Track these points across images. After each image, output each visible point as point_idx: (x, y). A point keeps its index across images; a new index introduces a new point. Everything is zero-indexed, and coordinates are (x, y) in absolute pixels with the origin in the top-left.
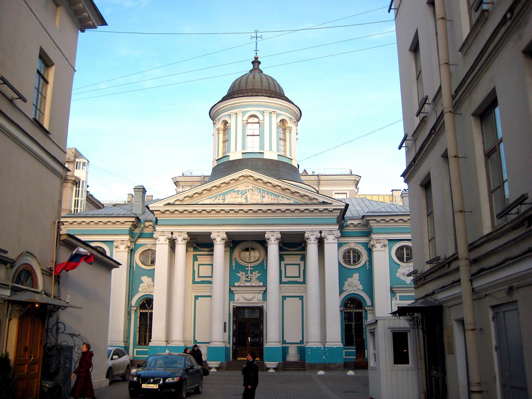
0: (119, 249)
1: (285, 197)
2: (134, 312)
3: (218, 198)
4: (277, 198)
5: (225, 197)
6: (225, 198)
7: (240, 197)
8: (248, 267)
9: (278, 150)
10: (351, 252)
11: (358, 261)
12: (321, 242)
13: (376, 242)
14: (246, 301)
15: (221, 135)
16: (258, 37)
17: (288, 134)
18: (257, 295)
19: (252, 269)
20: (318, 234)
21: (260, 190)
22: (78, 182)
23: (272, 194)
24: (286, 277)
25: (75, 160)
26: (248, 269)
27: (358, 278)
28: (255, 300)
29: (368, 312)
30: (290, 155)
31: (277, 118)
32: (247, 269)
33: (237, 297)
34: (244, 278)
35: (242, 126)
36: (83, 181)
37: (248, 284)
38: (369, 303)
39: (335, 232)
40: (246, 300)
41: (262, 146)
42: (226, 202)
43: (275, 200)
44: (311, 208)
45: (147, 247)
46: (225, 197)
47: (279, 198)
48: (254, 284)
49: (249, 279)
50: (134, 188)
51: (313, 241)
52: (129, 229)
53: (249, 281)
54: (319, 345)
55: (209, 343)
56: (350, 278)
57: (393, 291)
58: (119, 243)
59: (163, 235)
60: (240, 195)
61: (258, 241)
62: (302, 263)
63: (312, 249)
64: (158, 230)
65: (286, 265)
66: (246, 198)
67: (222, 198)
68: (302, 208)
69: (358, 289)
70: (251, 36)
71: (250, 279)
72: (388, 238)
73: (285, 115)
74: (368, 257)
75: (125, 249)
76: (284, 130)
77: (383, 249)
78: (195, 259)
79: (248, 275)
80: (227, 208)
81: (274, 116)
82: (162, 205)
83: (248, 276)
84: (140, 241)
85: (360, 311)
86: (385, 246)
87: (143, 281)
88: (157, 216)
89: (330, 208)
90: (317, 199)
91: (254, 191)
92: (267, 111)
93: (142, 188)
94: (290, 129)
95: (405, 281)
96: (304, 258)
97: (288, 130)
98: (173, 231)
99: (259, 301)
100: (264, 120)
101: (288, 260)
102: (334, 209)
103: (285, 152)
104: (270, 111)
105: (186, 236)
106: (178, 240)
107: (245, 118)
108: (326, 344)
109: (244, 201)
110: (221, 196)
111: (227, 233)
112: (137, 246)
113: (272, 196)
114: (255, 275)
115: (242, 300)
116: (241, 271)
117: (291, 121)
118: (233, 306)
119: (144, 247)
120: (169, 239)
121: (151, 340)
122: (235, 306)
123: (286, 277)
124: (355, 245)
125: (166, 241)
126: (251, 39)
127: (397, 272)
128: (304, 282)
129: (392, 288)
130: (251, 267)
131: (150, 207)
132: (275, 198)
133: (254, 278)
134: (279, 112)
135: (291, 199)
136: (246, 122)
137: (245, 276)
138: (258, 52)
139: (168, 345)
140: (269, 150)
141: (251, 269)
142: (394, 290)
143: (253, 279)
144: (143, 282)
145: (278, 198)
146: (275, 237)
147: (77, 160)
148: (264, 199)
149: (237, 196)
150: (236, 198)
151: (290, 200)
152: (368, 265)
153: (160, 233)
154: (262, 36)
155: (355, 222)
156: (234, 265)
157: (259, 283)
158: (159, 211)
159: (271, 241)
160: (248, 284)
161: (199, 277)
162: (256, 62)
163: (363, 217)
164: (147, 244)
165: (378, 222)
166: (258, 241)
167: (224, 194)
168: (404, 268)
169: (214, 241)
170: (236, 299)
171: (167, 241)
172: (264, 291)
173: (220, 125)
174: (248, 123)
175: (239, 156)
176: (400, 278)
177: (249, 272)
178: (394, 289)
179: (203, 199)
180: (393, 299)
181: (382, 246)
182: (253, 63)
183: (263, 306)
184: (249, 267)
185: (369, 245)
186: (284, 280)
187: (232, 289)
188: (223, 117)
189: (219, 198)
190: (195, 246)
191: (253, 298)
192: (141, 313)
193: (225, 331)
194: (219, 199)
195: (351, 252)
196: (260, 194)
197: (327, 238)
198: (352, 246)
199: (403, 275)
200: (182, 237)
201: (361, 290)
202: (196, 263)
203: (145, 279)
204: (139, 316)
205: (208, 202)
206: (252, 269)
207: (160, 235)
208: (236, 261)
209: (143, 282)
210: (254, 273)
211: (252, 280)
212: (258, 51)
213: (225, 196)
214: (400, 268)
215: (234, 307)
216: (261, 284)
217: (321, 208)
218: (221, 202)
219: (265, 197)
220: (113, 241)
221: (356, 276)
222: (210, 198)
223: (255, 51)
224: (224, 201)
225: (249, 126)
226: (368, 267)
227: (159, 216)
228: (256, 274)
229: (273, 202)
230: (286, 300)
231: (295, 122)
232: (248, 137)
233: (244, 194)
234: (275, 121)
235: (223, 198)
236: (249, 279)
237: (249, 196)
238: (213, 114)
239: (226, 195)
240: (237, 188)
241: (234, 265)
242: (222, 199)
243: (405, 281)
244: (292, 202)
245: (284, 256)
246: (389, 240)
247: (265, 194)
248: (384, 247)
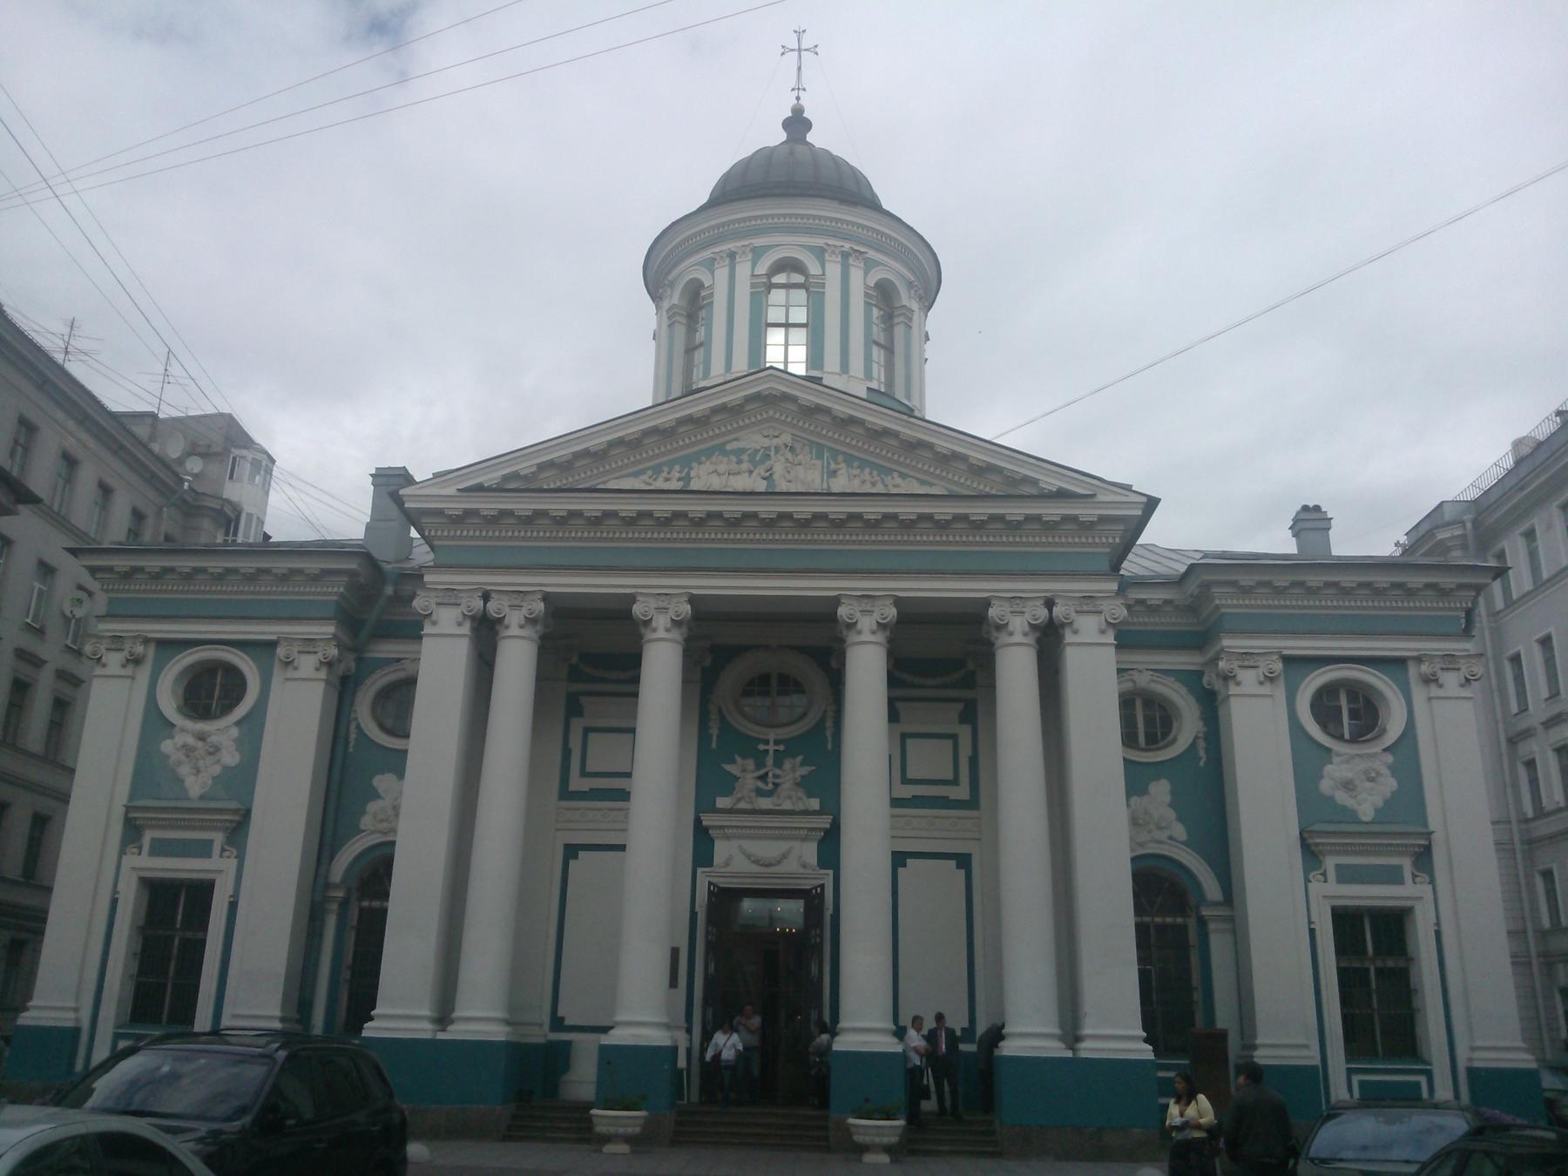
0: (296, 669)
1: (912, 473)
2: (334, 907)
3: (664, 474)
4: (882, 479)
5: (688, 473)
6: (692, 476)
7: (747, 474)
8: (767, 742)
9: (868, 375)
10: (1139, 704)
11: (1164, 737)
13: (1236, 663)
14: (755, 868)
15: (681, 331)
16: (806, 50)
17: (899, 331)
18: (797, 844)
19: (781, 748)
20: (1038, 609)
21: (819, 450)
22: (232, 516)
23: (863, 464)
24: (905, 781)
25: (227, 451)
26: (767, 747)
27: (1168, 799)
28: (790, 866)
29: (1212, 926)
30: (908, 397)
31: (866, 274)
32: (761, 747)
33: (722, 850)
34: (749, 781)
35: (752, 293)
36: (250, 516)
37: (765, 803)
38: (1212, 889)
39: (1105, 606)
40: (757, 862)
41: (815, 356)
42: (694, 486)
43: (874, 484)
44: (1015, 511)
45: (404, 670)
46: (688, 473)
47: (890, 478)
48: (787, 806)
49: (767, 784)
50: (374, 472)
51: (1018, 638)
52: (335, 598)
53: (769, 794)
54: (1055, 1049)
55: (605, 1030)
56: (1139, 796)
57: (1313, 848)
58: (296, 649)
59: (452, 601)
60: (745, 466)
61: (803, 650)
62: (964, 732)
64: (431, 583)
65: (904, 737)
66: (768, 474)
67: (677, 475)
68: (979, 511)
69: (1171, 838)
70: (783, 47)
71: (773, 783)
72: (1286, 652)
73: (892, 270)
74: (1201, 724)
75: (317, 669)
76: (888, 319)
77: (1266, 689)
78: (574, 708)
79: (766, 770)
80: (698, 508)
82: (451, 491)
83: (767, 774)
84: (386, 649)
85: (1179, 920)
86: (1271, 680)
87: (380, 791)
88: (433, 533)
89: (1085, 512)
90: (1034, 482)
91: (798, 450)
92: (833, 248)
93: (402, 472)
94: (908, 314)
95: (1354, 812)
97: (901, 319)
98: (489, 588)
99: (804, 867)
100: (824, 274)
102: (1103, 519)
103: (890, 381)
104: (844, 249)
105: (540, 607)
106: (506, 621)
107: (762, 269)
108: (1084, 1045)
109: (761, 486)
110: (677, 468)
111: (693, 600)
112: (366, 667)
113: (862, 471)
114: (793, 769)
115: (741, 865)
116: (740, 756)
117: (909, 292)
118: (710, 883)
119: (392, 669)
120: (473, 618)
121: (373, 1013)
122: (715, 885)
123: (905, 781)
124: (1155, 678)
125: (459, 624)
126: (783, 54)
127: (1322, 777)
128: (973, 803)
129: (1306, 835)
130: (777, 742)
131: (404, 499)
132: (878, 478)
133: (787, 785)
134: (872, 254)
135: (934, 481)
136: (765, 280)
137: (753, 772)
138: (802, 94)
139: (441, 1036)
140: (837, 370)
141: (777, 748)
142: (1317, 845)
143: (787, 786)
144: (378, 797)
145: (888, 480)
146: (876, 616)
147: (236, 452)
148: (832, 480)
149: (734, 466)
150: (729, 474)
151: (931, 485)
152: (1202, 753)
153: (441, 594)
154: (816, 46)
155: (1155, 596)
156: (714, 732)
157: (805, 799)
158: (439, 513)
159: (859, 632)
160: (765, 803)
161: (584, 774)
162: (797, 124)
163: (1192, 567)
164: (403, 659)
165: (1246, 591)
166: (803, 650)
167: (686, 462)
168: (1347, 762)
169: (643, 630)
170: (719, 857)
171: (466, 629)
172: (827, 832)
173: (675, 298)
174: (771, 286)
176: (1332, 798)
177: (768, 758)
178: (1318, 841)
179: (611, 477)
180: (1311, 877)
181: (1262, 679)
182: (787, 124)
183: (822, 886)
184: (771, 742)
185: (1205, 679)
187: (708, 820)
188: (691, 270)
189: (669, 473)
190: (575, 660)
191: (784, 856)
192: (362, 910)
193: (673, 983)
194: (668, 476)
195: (1139, 704)
196: (819, 463)
197: (1076, 625)
198: (1143, 680)
199: (1347, 788)
200: (524, 611)
201: (1182, 843)
202: (577, 725)
203: (382, 782)
204: (355, 923)
206: (781, 748)
207: (439, 600)
208: (722, 719)
209: (378, 797)
210: (787, 764)
211: (779, 789)
212: (804, 90)
213: (692, 469)
214: (1331, 763)
215: (712, 888)
216: (815, 804)
217: (1053, 511)
218: (675, 485)
219: (840, 472)
220: (272, 645)
221: (1161, 790)
222: (636, 475)
223: (793, 89)
224: (689, 483)
225: (777, 296)
226: (1204, 759)
227: (439, 533)
228: (793, 770)
229: (868, 489)
230: (905, 865)
231: (921, 298)
232: (769, 329)
233: (762, 462)
235: (684, 474)
236: (771, 786)
237: (779, 469)
238: (656, 275)
239: (695, 465)
240: (737, 439)
241: (714, 732)
242: (679, 480)
243: (1353, 811)
245: (899, 705)
246: (1288, 660)
247: (837, 464)
248: (1268, 685)
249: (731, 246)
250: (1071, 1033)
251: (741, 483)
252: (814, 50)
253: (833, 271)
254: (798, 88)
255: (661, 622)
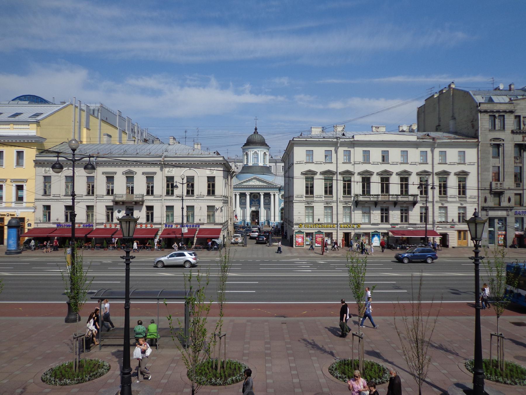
12: (274, 195)
63: (272, 197)
81: (262, 151)
96: (270, 198)
101: (266, 198)
107: (254, 152)
128: (270, 204)
162: (256, 129)
175: (252, 165)
182: (255, 129)
186: (265, 203)
205: (244, 184)
218: (248, 184)
228: (257, 202)
234: (262, 153)
244: (267, 185)
249: (250, 150)
250: (274, 220)
251: (253, 184)
252: (258, 119)
253: (260, 153)
254: (256, 124)
255: (248, 194)
